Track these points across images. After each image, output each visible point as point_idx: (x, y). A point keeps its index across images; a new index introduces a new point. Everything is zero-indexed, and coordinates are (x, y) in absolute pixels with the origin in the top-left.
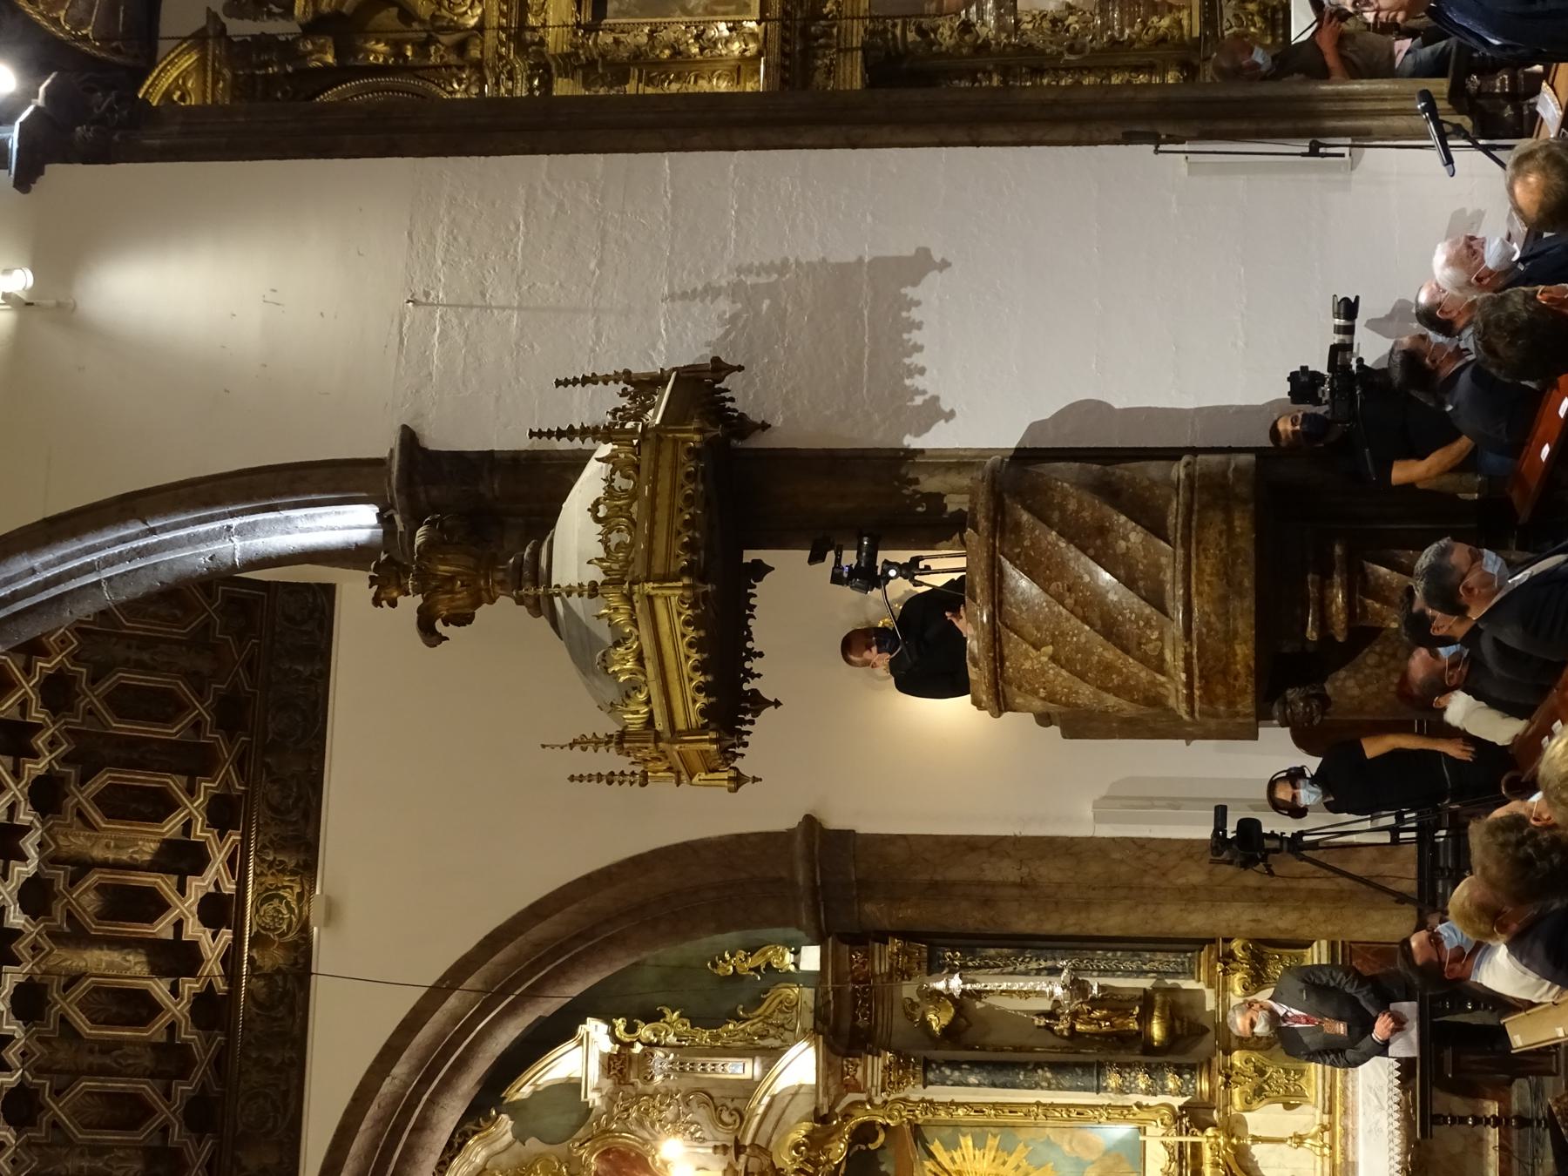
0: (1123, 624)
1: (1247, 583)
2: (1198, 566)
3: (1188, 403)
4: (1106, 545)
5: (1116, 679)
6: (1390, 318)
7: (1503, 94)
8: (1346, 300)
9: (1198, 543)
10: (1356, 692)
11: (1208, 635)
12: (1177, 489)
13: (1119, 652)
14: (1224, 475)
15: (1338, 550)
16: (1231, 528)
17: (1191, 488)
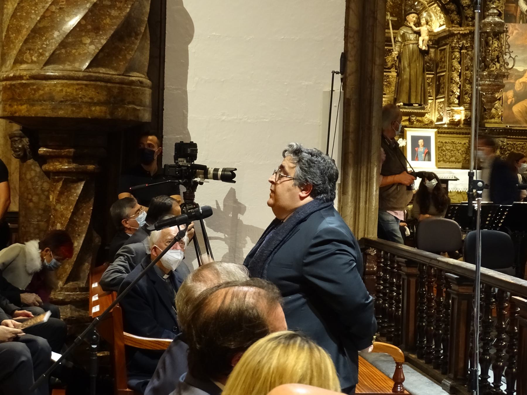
0: (41, 39)
1: (61, 113)
2: (73, 84)
3: (190, 87)
4: (88, 32)
5: (13, 36)
6: (236, 201)
7: (365, 267)
8: (234, 175)
9: (86, 85)
10: (28, 177)
11: (32, 89)
12: (123, 75)
13: (25, 37)
15: (91, 167)
16: (95, 104)
17: (122, 83)
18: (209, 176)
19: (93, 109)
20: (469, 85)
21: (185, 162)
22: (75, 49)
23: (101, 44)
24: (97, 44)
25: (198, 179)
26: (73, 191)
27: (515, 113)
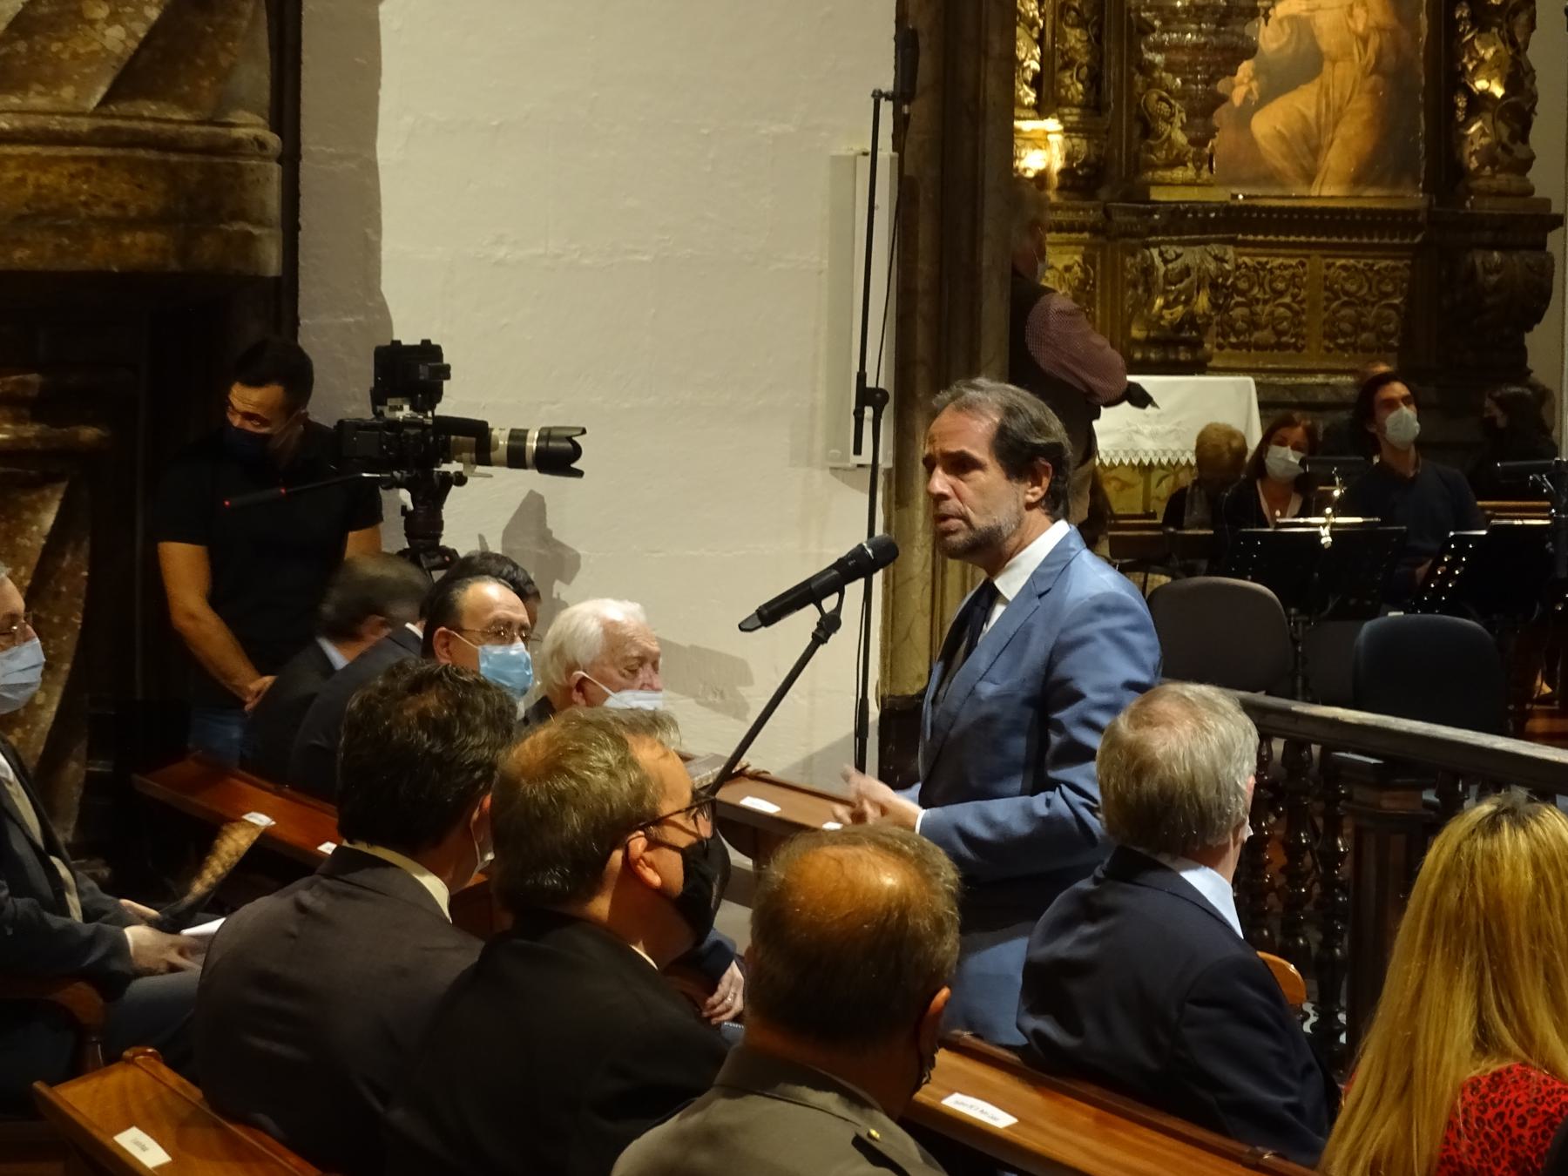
2: (57, 160)
3: (388, 149)
6: (546, 538)
8: (577, 452)
9: (102, 161)
12: (211, 122)
14: (239, 215)
15: (89, 433)
16: (133, 224)
18: (493, 455)
19: (127, 240)
20: (1077, 32)
21: (406, 407)
22: (59, 40)
23: (145, 19)
24: (132, 20)
25: (453, 467)
26: (27, 515)
27: (1262, 143)
